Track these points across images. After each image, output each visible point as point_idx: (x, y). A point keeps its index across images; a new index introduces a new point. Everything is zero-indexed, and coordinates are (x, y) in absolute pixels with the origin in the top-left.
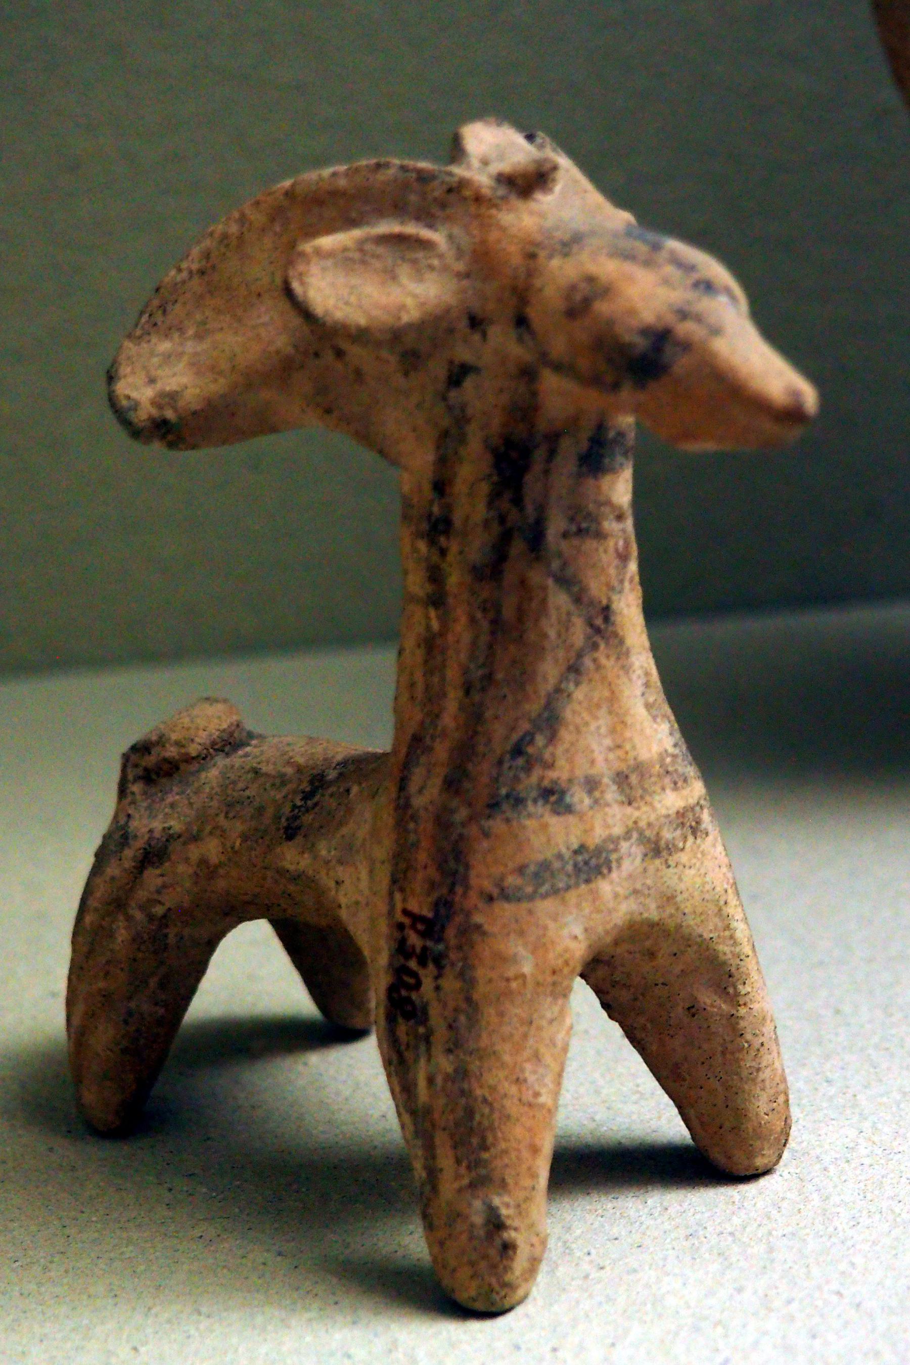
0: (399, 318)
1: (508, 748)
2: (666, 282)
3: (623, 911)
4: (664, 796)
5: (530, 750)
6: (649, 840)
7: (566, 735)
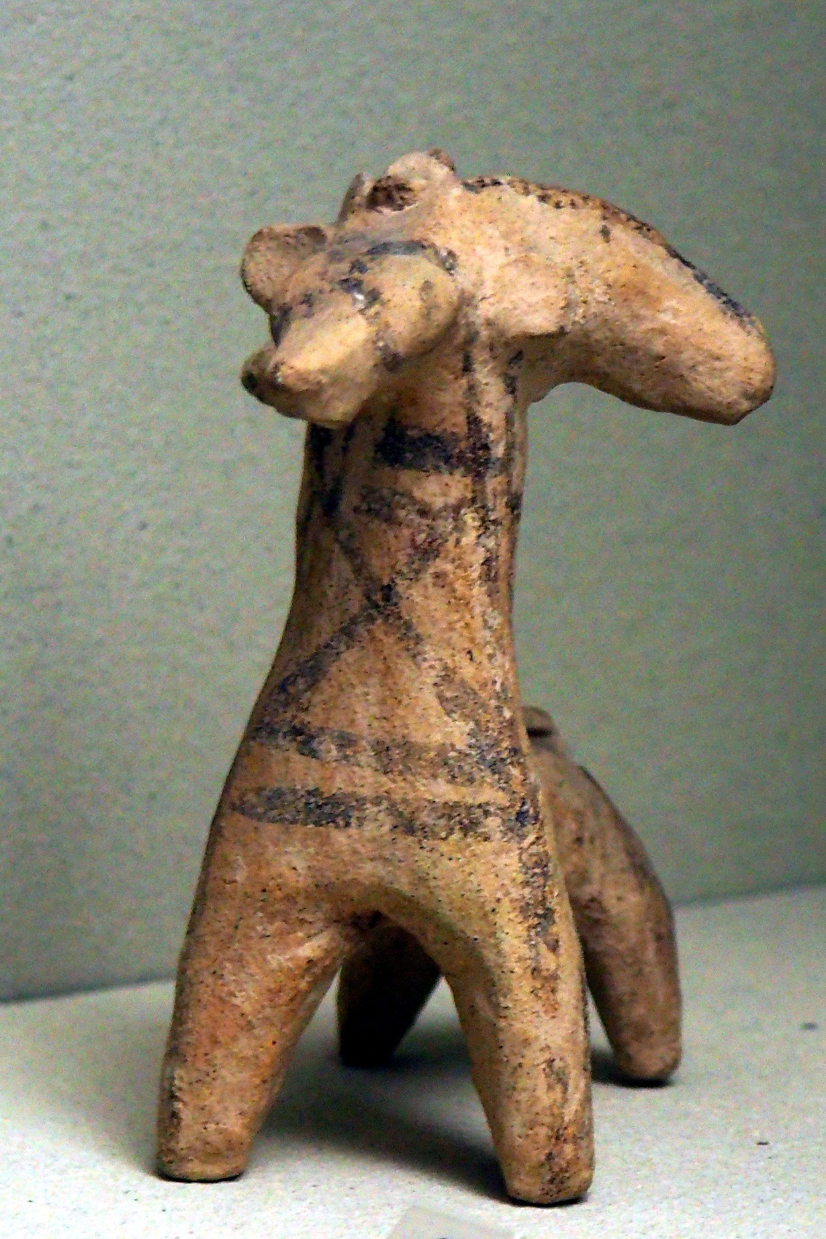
4: (431, 781)
5: (291, 689)
6: (401, 814)
7: (327, 690)
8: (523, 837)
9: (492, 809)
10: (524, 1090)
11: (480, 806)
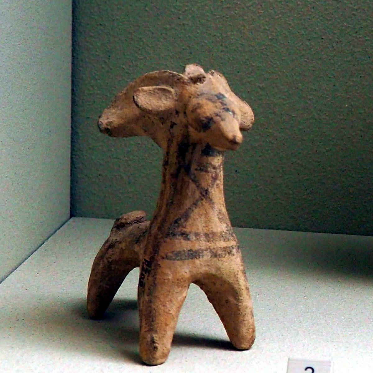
0: (159, 109)
1: (173, 221)
2: (216, 107)
3: (204, 269)
5: (179, 222)
6: (213, 252)
7: (190, 221)
8: (239, 253)
9: (234, 247)
10: (246, 320)
11: (231, 247)
